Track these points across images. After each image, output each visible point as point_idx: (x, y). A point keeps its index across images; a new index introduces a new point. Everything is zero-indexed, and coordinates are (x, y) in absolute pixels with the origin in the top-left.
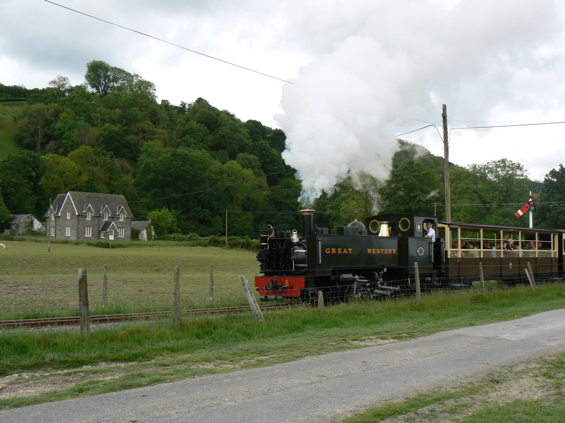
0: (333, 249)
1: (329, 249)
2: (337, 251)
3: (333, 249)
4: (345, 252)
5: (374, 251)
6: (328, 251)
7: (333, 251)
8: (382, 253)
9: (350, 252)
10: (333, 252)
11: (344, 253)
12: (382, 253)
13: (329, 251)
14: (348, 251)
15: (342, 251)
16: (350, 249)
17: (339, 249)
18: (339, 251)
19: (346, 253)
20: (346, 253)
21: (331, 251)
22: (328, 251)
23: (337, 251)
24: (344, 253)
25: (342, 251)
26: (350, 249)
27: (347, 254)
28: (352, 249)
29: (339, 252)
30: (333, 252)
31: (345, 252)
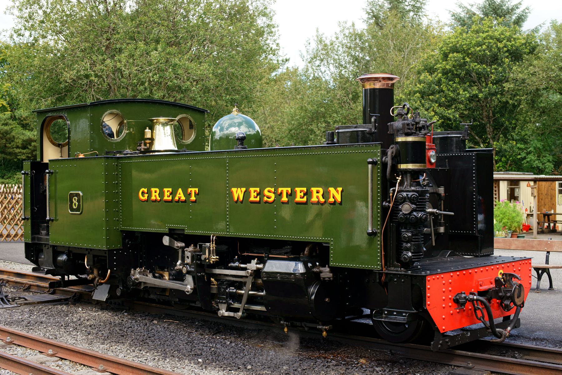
0: (153, 190)
1: (146, 190)
2: (161, 194)
3: (153, 190)
4: (179, 198)
5: (253, 194)
6: (143, 193)
7: (154, 194)
8: (285, 199)
9: (193, 198)
10: (153, 198)
11: (177, 198)
12: (285, 199)
13: (146, 195)
14: (188, 195)
15: (173, 194)
16: (193, 190)
17: (166, 190)
18: (167, 194)
19: (183, 198)
20: (183, 198)
21: (149, 193)
22: (143, 193)
23: (161, 194)
24: (177, 198)
25: (173, 194)
26: (193, 190)
27: (185, 201)
28: (197, 189)
29: (166, 198)
31: (179, 198)
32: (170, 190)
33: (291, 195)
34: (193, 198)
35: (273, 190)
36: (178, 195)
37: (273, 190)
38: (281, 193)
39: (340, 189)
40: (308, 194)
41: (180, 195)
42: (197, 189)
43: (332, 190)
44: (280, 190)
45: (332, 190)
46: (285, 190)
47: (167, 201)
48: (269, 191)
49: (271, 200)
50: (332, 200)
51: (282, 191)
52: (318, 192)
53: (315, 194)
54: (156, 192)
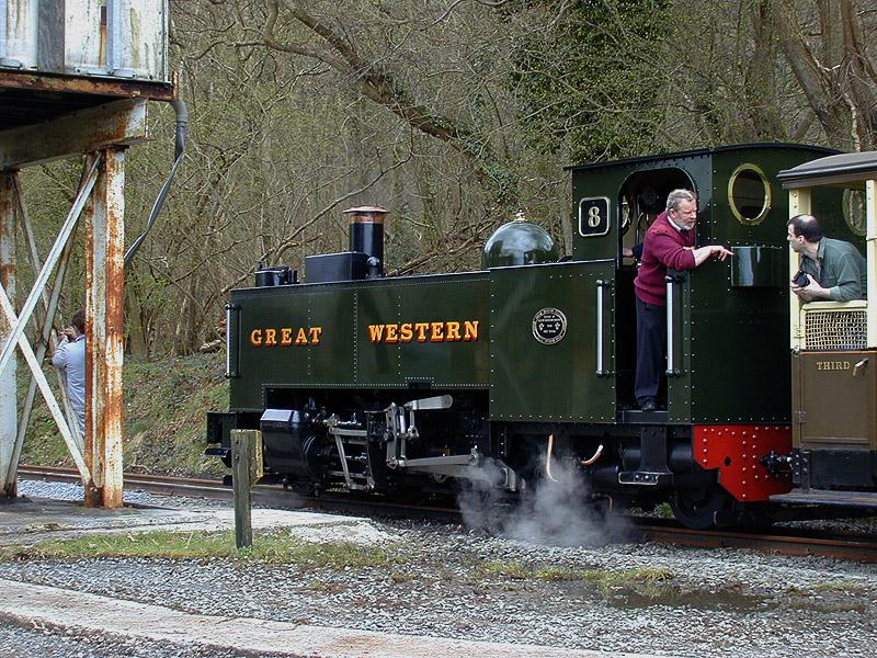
2: (279, 336)
4: (301, 340)
7: (269, 337)
8: (422, 337)
9: (316, 340)
10: (268, 342)
12: (422, 337)
15: (293, 335)
16: (316, 330)
18: (285, 336)
22: (256, 336)
23: (279, 336)
24: (298, 341)
25: (293, 335)
28: (320, 329)
30: (268, 342)
32: (290, 330)
33: (429, 332)
34: (316, 340)
35: (410, 326)
36: (299, 337)
37: (410, 326)
38: (419, 327)
39: (476, 323)
40: (445, 330)
41: (302, 337)
42: (320, 329)
43: (467, 323)
44: (417, 325)
45: (467, 323)
46: (422, 326)
47: (286, 345)
48: (406, 328)
49: (410, 337)
50: (467, 336)
51: (419, 327)
52: (454, 327)
53: (450, 330)
54: (271, 334)
